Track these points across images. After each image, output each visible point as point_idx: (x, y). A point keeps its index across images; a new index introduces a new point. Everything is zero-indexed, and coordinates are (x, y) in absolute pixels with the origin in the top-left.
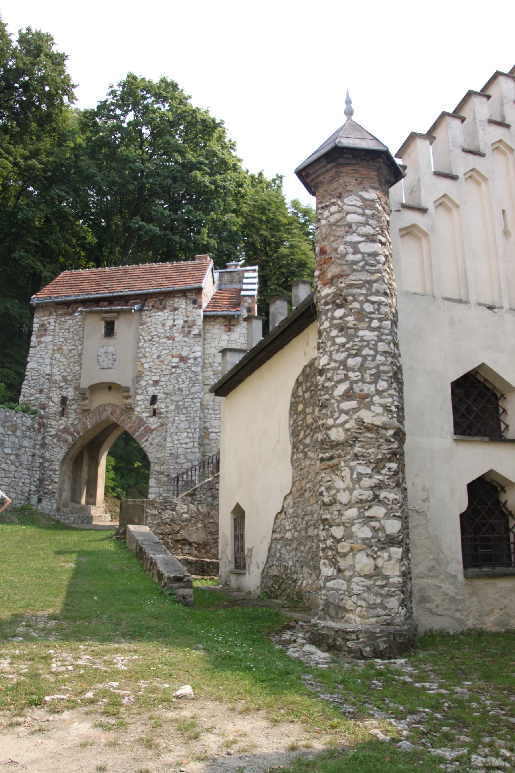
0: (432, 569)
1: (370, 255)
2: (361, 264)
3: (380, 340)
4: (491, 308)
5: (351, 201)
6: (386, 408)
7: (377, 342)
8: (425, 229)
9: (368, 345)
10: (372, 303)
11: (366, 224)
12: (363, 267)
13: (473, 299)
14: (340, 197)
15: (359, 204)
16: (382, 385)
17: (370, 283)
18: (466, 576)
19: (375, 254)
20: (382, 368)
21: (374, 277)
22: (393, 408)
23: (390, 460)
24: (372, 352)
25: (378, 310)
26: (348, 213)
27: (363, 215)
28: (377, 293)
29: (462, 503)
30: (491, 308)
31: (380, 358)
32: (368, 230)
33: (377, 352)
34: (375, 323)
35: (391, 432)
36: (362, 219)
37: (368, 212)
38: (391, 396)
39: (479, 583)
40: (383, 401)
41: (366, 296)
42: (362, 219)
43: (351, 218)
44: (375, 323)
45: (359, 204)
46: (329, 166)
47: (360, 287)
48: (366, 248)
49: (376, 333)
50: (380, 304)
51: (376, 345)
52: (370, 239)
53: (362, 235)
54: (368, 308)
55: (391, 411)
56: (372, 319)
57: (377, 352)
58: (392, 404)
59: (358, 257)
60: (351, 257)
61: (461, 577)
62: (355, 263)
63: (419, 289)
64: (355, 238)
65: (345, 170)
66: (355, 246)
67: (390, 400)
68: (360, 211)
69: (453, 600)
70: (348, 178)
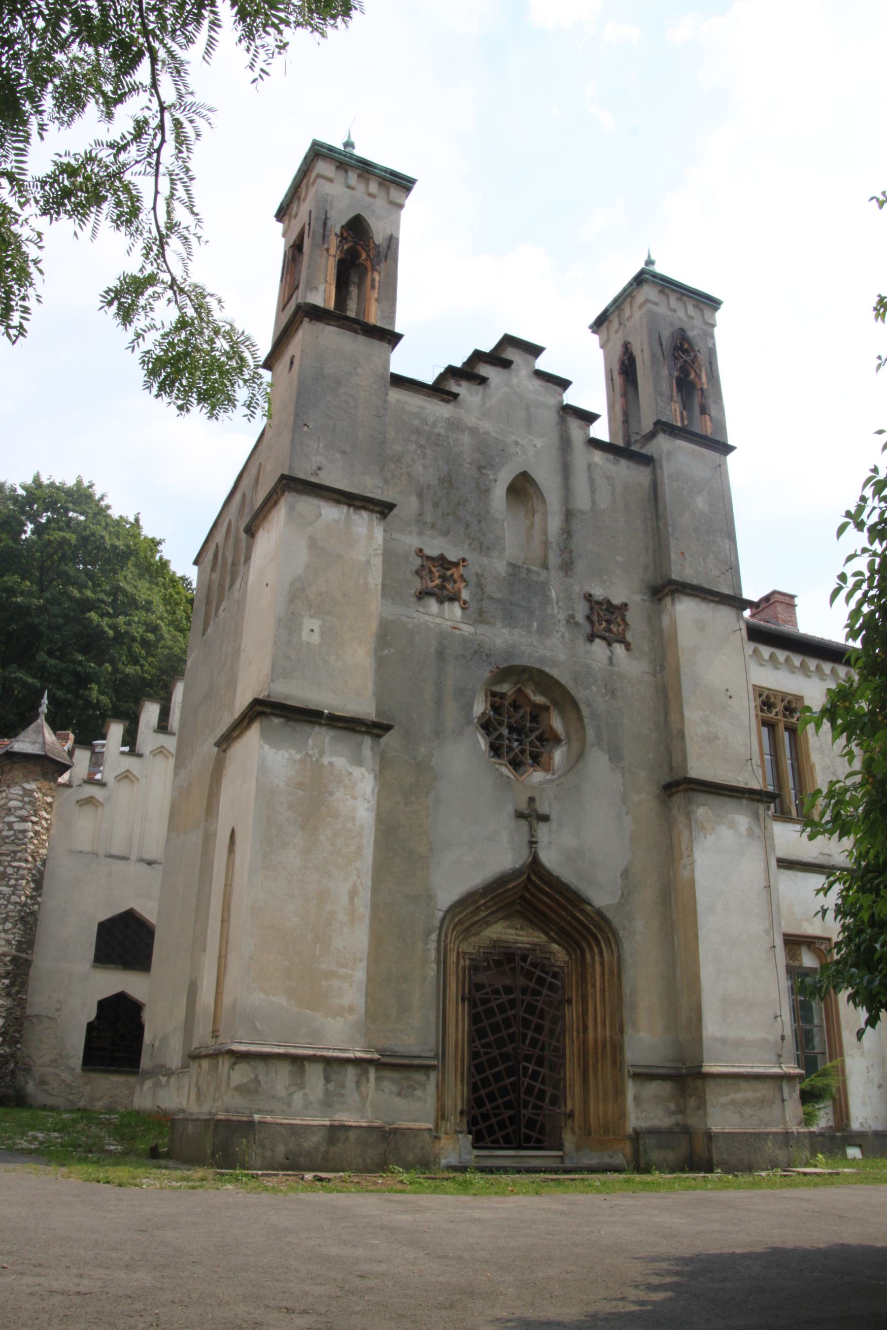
0: (55, 1061)
1: (20, 831)
2: (12, 838)
3: (13, 893)
4: (150, 863)
5: (16, 790)
6: (8, 942)
7: (10, 895)
8: (101, 800)
9: (3, 898)
10: (13, 867)
11: (21, 808)
12: (13, 841)
13: (134, 856)
14: (9, 787)
15: (21, 793)
16: (9, 925)
17: (15, 852)
18: (83, 1070)
19: (25, 831)
20: (11, 914)
21: (19, 848)
22: (13, 942)
23: (5, 978)
24: (6, 902)
25: (17, 873)
26: (10, 800)
27: (22, 801)
28: (20, 860)
29: (91, 1014)
30: (150, 863)
31: (11, 907)
32: (23, 813)
33: (9, 902)
34: (12, 882)
35: (8, 958)
36: (20, 804)
37: (26, 799)
38: (14, 934)
39: (93, 1075)
40: (7, 937)
41: (10, 862)
42: (20, 804)
43: (12, 804)
44: (12, 882)
45: (21, 793)
46: (8, 761)
47: (7, 855)
48: (18, 826)
49: (12, 889)
50: (19, 868)
51: (9, 898)
52: (24, 819)
53: (18, 817)
54: (10, 871)
55: (11, 944)
56: (10, 879)
57: (9, 902)
58: (13, 939)
59: (12, 832)
60: (5, 833)
61: (79, 1069)
62: (8, 837)
63: (87, 847)
64: (12, 819)
65: (16, 766)
66: (10, 825)
67: (12, 936)
68: (20, 798)
69: (68, 1085)
70: (18, 774)
